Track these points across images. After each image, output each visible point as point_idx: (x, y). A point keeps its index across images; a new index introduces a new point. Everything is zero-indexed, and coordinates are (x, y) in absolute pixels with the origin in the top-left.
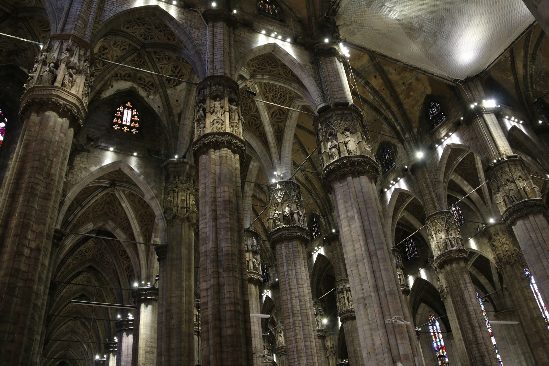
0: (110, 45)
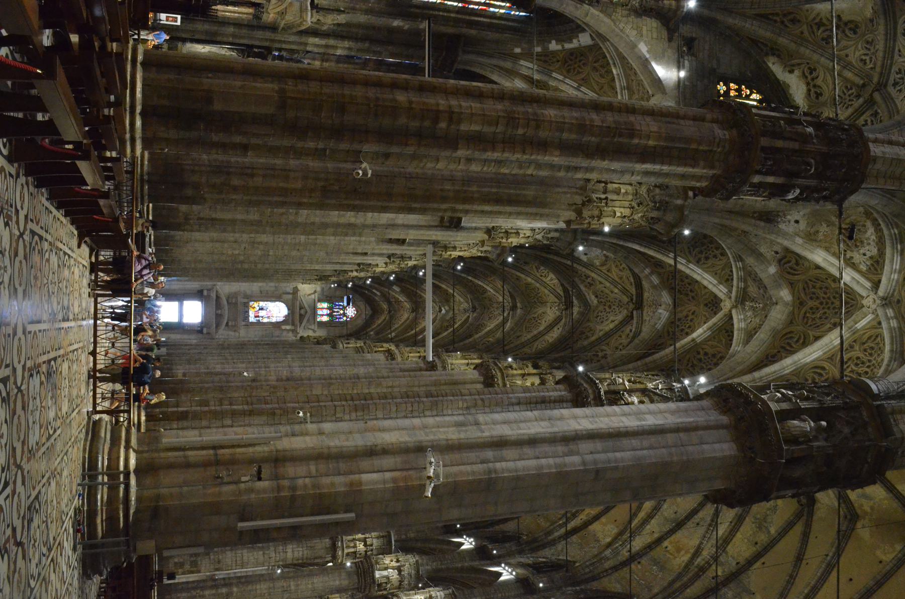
0: (864, 35)
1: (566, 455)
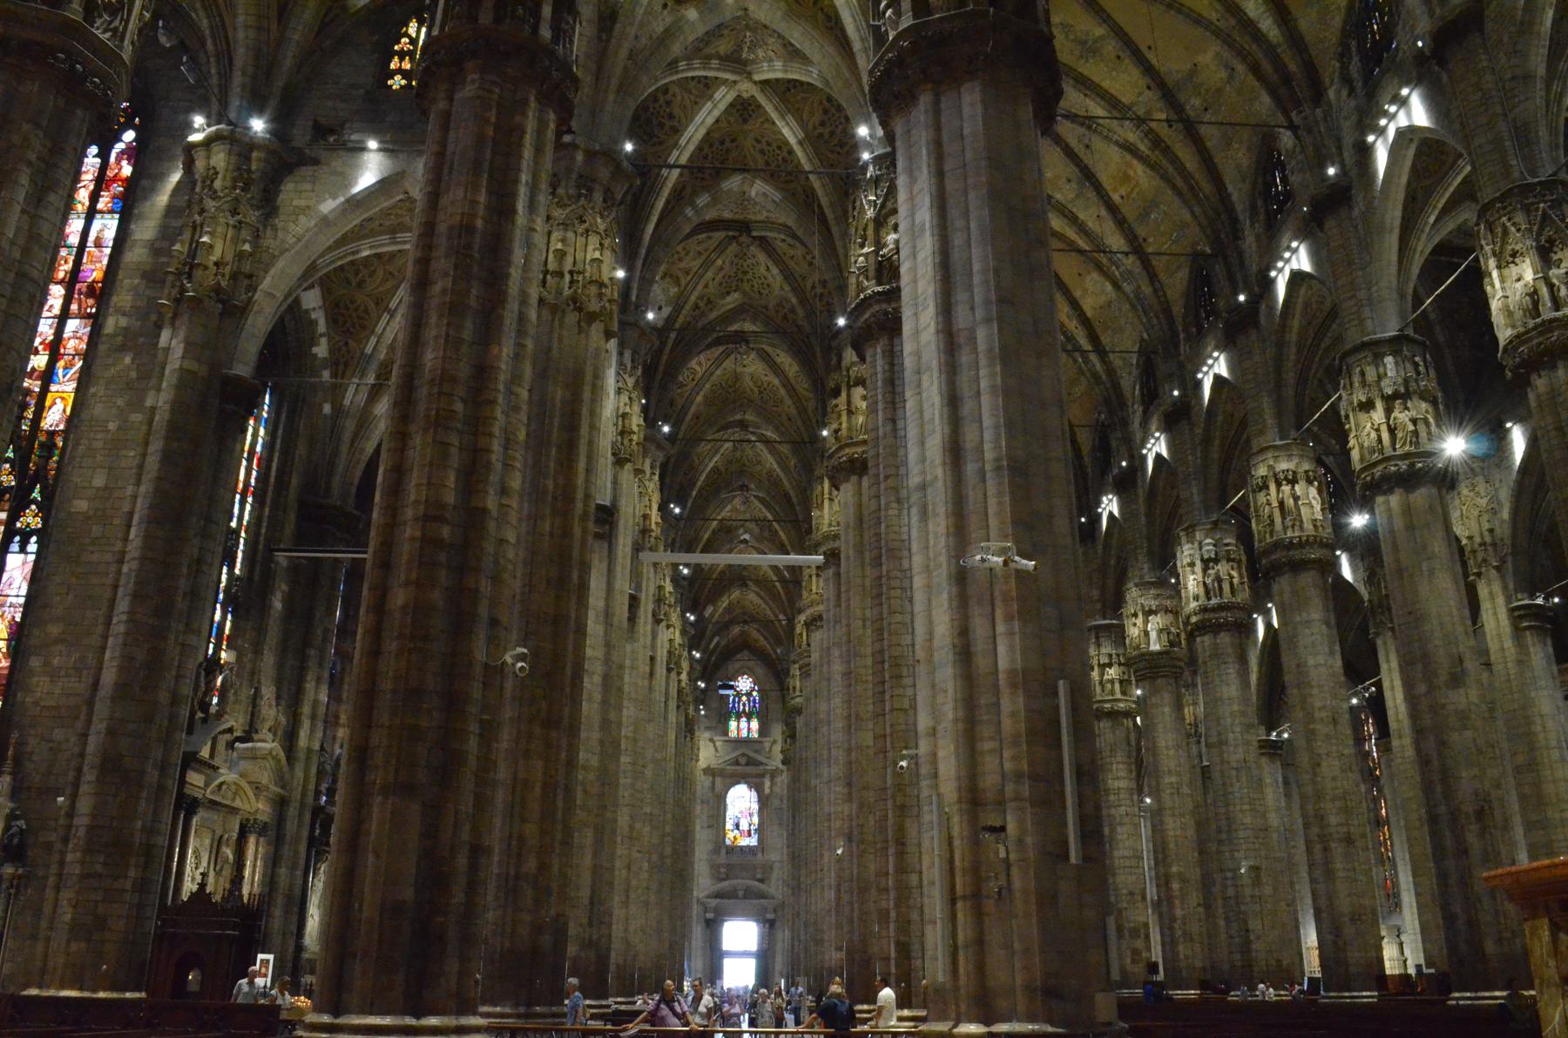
1: (975, 350)
